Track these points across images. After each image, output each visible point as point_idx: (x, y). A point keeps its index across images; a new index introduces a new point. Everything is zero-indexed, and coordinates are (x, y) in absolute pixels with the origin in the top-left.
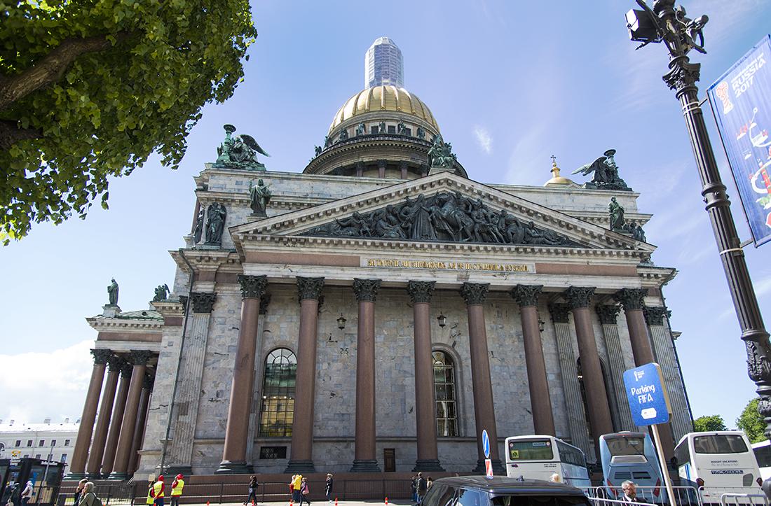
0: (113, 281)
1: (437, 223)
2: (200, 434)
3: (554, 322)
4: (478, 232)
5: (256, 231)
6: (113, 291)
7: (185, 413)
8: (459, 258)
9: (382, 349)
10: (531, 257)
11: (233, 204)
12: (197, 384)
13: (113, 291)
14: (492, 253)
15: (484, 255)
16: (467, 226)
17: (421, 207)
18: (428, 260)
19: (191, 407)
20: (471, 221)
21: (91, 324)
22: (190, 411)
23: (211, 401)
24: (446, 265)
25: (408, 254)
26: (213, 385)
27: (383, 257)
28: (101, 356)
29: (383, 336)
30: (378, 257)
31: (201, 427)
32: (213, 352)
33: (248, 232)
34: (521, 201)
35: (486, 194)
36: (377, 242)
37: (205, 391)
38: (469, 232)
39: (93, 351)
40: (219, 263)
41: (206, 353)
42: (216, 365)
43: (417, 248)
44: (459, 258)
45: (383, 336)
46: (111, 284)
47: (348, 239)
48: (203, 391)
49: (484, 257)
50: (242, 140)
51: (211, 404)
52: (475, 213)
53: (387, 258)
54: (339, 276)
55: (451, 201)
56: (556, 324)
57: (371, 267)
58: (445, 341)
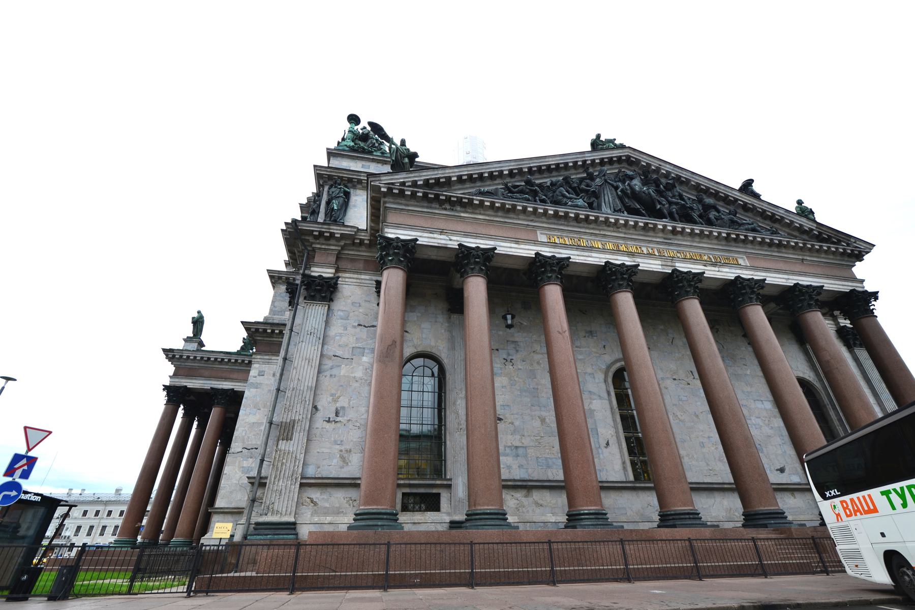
0: (199, 312)
2: (311, 471)
5: (403, 184)
6: (198, 323)
7: (288, 438)
11: (359, 186)
12: (309, 396)
13: (198, 323)
19: (297, 427)
21: (167, 356)
22: (296, 435)
23: (329, 421)
25: (597, 232)
26: (330, 399)
28: (175, 395)
31: (311, 459)
32: (331, 354)
33: (393, 184)
37: (319, 407)
39: (166, 388)
40: (342, 243)
41: (322, 355)
42: (334, 372)
44: (658, 243)
46: (196, 315)
48: (315, 408)
50: (369, 128)
51: (327, 426)
54: (513, 250)
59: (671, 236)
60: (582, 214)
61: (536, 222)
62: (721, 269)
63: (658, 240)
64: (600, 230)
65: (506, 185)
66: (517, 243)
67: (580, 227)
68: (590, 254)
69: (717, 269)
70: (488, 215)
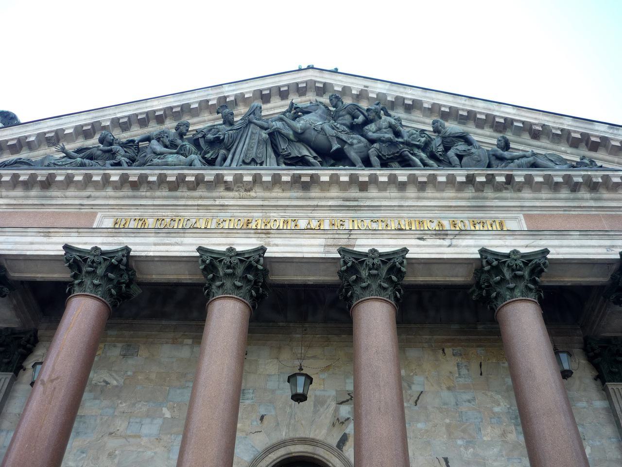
1: (283, 145)
3: (603, 383)
4: (379, 157)
8: (331, 208)
9: (149, 453)
10: (509, 199)
14: (411, 192)
15: (392, 197)
16: (351, 145)
17: (250, 122)
18: (257, 214)
20: (363, 139)
24: (253, 141)
27: (150, 212)
29: (159, 421)
30: (137, 213)
34: (473, 102)
35: (397, 98)
36: (134, 174)
38: (353, 155)
43: (228, 187)
44: (331, 208)
45: (159, 421)
47: (70, 172)
49: (395, 203)
52: (372, 127)
53: (161, 213)
55: (319, 112)
56: (611, 386)
57: (117, 229)
58: (320, 434)
59: (354, 193)
60: (172, 175)
61: (96, 198)
62: (455, 242)
63: (330, 203)
64: (214, 198)
65: (63, 150)
66: (47, 235)
67: (176, 198)
68: (179, 240)
69: (447, 242)
70: (15, 198)
